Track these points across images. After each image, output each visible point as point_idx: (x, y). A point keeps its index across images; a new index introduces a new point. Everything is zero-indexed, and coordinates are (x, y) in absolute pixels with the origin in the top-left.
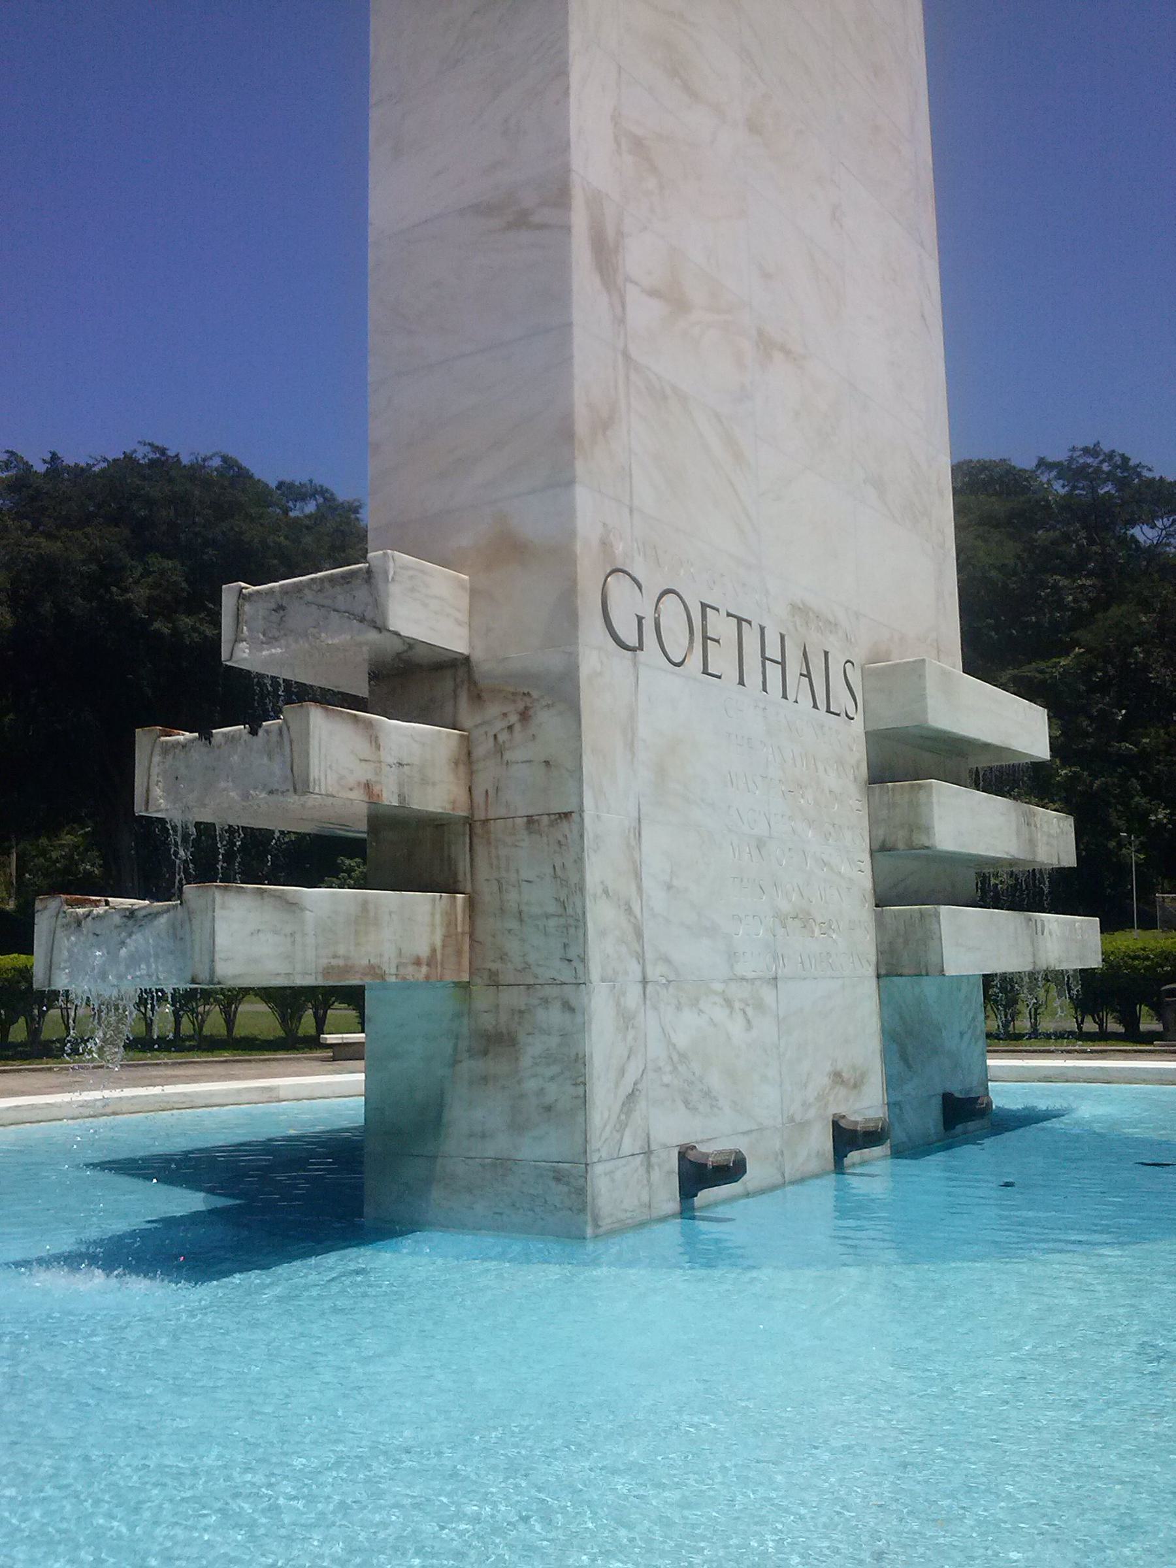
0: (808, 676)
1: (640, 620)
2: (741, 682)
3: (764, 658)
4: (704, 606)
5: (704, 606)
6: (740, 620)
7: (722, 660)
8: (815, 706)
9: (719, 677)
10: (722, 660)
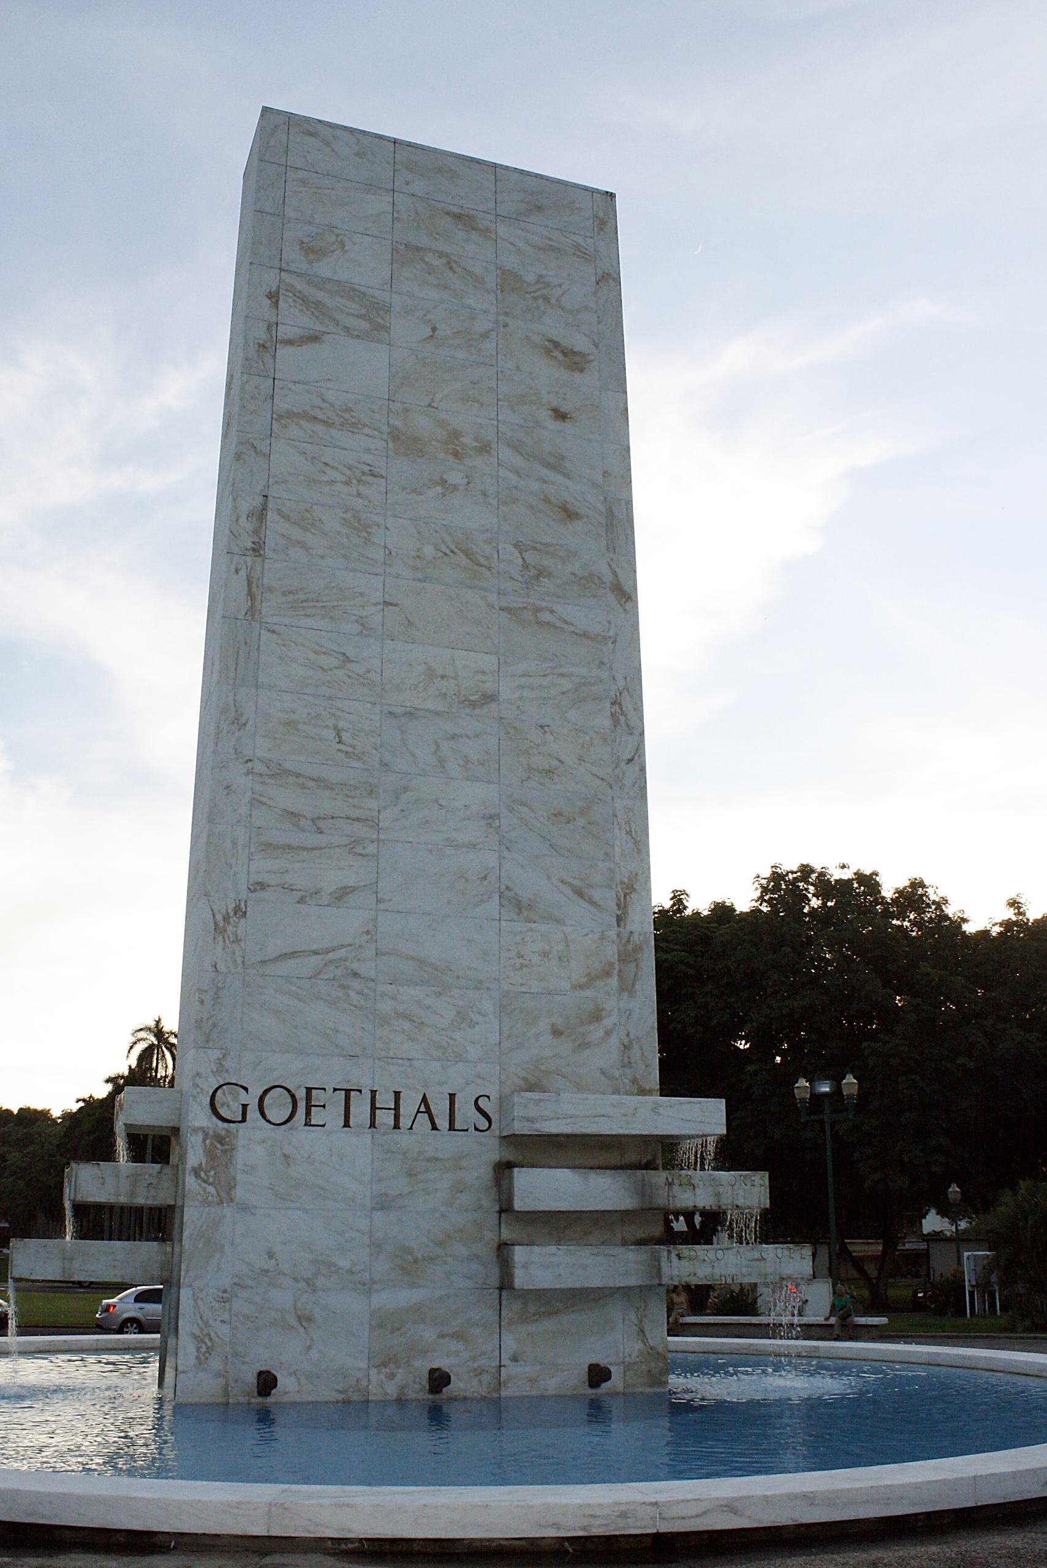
0: (428, 1111)
1: (245, 1106)
2: (347, 1124)
3: (373, 1108)
4: (309, 1090)
5: (309, 1090)
6: (348, 1092)
8: (434, 1127)
9: (323, 1126)
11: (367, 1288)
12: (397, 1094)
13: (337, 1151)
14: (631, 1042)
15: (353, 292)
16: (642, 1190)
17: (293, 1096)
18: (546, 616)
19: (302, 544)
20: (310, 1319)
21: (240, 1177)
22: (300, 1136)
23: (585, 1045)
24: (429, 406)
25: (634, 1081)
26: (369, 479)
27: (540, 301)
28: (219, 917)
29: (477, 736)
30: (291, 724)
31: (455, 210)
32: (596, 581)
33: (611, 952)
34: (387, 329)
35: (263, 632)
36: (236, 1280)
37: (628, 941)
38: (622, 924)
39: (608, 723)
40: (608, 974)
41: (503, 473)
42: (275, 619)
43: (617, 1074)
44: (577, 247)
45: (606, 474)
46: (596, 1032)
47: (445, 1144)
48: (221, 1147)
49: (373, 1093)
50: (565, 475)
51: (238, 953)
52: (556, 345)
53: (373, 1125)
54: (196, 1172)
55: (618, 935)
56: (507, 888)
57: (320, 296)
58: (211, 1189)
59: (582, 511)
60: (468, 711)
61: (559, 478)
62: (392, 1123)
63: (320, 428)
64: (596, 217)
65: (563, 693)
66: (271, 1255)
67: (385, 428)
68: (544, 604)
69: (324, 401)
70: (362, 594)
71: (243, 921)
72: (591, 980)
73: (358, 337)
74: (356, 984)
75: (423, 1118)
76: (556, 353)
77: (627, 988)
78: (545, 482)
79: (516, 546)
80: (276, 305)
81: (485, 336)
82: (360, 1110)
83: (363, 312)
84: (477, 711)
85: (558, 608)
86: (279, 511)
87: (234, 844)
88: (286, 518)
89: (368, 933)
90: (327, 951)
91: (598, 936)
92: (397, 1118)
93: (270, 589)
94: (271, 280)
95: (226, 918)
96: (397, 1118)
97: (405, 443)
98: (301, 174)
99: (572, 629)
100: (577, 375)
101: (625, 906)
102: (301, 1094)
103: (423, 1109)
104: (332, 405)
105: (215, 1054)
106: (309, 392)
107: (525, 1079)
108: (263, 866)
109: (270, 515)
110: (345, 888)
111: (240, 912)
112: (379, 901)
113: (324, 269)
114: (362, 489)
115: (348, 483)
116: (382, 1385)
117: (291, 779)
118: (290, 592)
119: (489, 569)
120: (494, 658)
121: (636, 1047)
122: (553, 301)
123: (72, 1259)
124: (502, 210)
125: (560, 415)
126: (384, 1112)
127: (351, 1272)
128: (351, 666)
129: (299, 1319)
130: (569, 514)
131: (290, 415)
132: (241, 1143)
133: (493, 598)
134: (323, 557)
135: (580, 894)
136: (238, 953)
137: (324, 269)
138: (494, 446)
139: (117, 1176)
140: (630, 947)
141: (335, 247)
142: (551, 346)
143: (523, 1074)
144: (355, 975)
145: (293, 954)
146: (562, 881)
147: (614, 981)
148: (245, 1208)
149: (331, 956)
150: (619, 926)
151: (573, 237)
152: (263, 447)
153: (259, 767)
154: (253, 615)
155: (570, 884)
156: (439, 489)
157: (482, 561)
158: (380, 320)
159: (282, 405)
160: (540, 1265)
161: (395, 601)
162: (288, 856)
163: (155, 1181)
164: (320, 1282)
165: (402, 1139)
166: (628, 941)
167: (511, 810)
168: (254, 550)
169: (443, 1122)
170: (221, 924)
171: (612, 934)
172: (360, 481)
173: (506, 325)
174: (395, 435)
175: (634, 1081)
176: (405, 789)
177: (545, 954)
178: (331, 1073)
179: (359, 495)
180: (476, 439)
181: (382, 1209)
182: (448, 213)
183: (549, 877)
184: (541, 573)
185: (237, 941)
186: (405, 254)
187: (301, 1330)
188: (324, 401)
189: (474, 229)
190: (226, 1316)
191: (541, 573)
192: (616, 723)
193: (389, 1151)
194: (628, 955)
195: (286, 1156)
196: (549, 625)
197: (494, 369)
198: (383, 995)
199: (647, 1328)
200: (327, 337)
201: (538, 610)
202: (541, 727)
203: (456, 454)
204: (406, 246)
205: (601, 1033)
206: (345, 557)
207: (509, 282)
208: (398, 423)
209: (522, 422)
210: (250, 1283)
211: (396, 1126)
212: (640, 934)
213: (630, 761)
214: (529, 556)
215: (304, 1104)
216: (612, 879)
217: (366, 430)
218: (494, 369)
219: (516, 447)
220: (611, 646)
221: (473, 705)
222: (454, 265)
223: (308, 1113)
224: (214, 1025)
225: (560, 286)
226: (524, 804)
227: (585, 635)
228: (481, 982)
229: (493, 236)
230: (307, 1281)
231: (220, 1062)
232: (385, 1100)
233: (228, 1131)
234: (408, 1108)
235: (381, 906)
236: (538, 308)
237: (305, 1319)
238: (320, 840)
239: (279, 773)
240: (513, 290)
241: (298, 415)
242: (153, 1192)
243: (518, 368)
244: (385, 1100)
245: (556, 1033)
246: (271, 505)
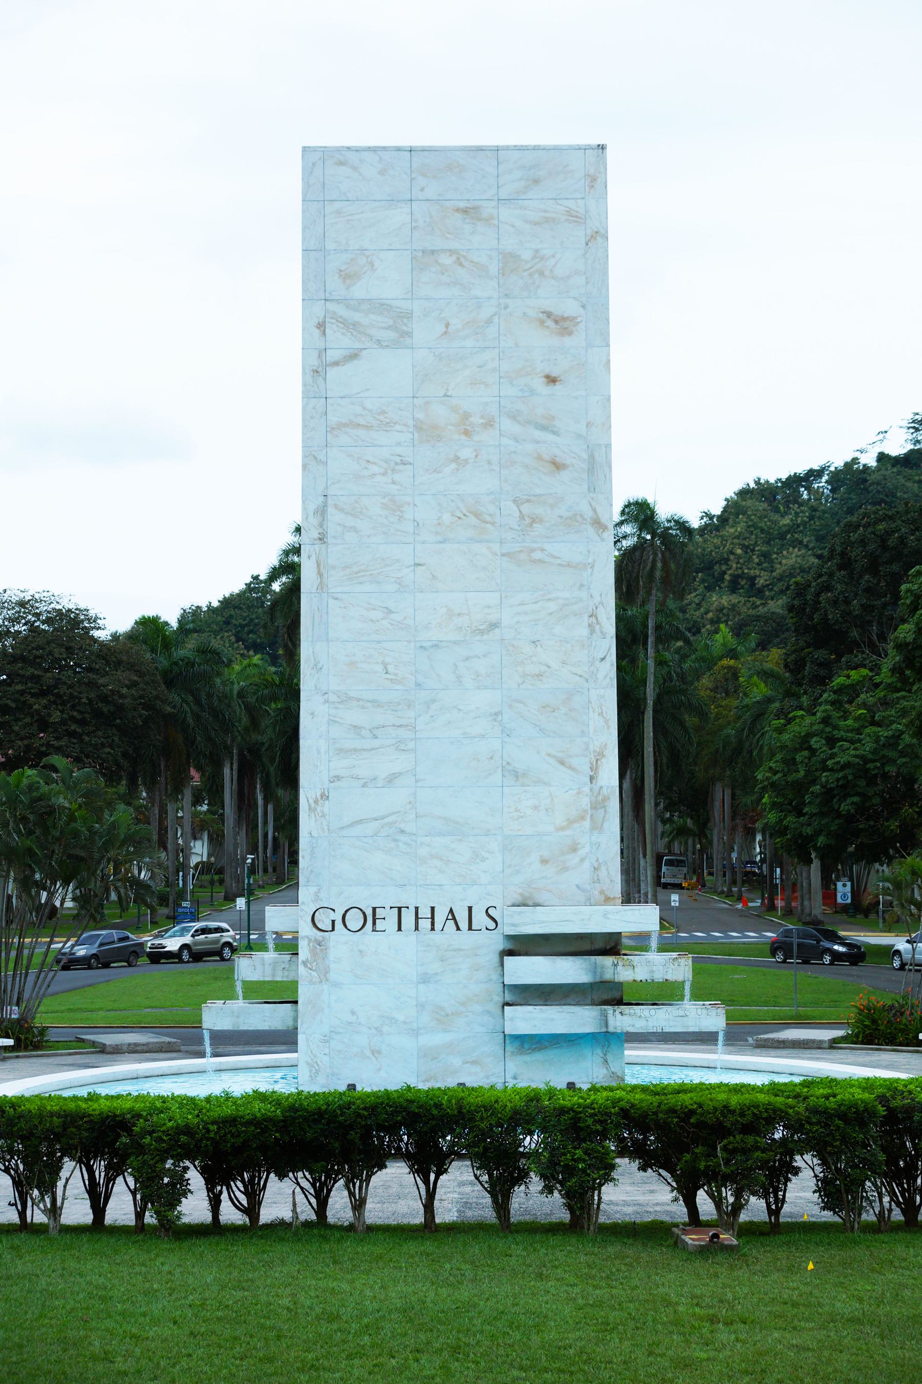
0: (454, 918)
1: (333, 922)
2: (400, 929)
3: (417, 918)
5: (374, 909)
6: (400, 909)
7: (388, 923)
8: (458, 929)
10: (388, 923)
11: (416, 1033)
12: (433, 909)
13: (393, 947)
14: (599, 865)
15: (381, 307)
16: (594, 969)
17: (364, 913)
18: (537, 555)
19: (354, 529)
20: (379, 1052)
21: (332, 966)
23: (566, 869)
24: (445, 395)
25: (602, 892)
26: (401, 467)
27: (536, 276)
28: (311, 801)
29: (484, 656)
30: (352, 664)
31: (462, 205)
32: (579, 518)
33: (585, 802)
34: (409, 334)
35: (331, 601)
36: (332, 1029)
37: (599, 793)
38: (594, 781)
39: (585, 632)
40: (583, 818)
41: (505, 441)
42: (339, 589)
43: (588, 887)
44: (569, 213)
45: (588, 425)
46: (573, 860)
47: (465, 938)
49: (417, 908)
50: (554, 433)
51: (325, 823)
52: (549, 314)
53: (417, 928)
54: (305, 963)
55: (591, 790)
56: (508, 763)
57: (357, 317)
58: (314, 974)
59: (568, 462)
60: (478, 638)
61: (550, 437)
62: (429, 927)
63: (361, 432)
64: (587, 175)
65: (551, 614)
66: (353, 1013)
67: (411, 423)
68: (535, 546)
69: (364, 408)
70: (398, 561)
71: (327, 802)
72: (571, 822)
73: (387, 346)
74: (403, 838)
75: (451, 923)
76: (550, 323)
77: (597, 827)
78: (538, 442)
79: (514, 501)
80: (324, 333)
81: (489, 321)
82: (408, 919)
83: (391, 323)
84: (485, 637)
85: (546, 546)
86: (336, 506)
87: (319, 752)
88: (341, 510)
89: (410, 803)
90: (383, 818)
91: (575, 792)
92: (433, 924)
93: (334, 567)
94: (318, 310)
95: (316, 802)
96: (433, 924)
97: (427, 432)
98: (337, 205)
99: (558, 561)
100: (567, 341)
101: (597, 768)
102: (369, 913)
103: (450, 917)
104: (370, 411)
105: (313, 889)
106: (353, 404)
107: (521, 894)
109: (330, 510)
110: (394, 774)
111: (325, 797)
112: (417, 781)
114: (397, 477)
115: (384, 474)
117: (354, 703)
118: (347, 567)
119: (493, 524)
120: (497, 595)
121: (603, 869)
122: (547, 273)
123: (238, 1017)
124: (503, 194)
125: (552, 380)
127: (405, 1023)
128: (392, 616)
129: (373, 1052)
130: (557, 466)
131: (341, 426)
132: (331, 944)
133: (496, 547)
134: (369, 536)
135: (562, 763)
136: (325, 823)
137: (358, 291)
138: (497, 420)
139: (264, 965)
140: (600, 798)
141: (366, 268)
142: (544, 317)
143: (520, 891)
144: (402, 831)
145: (360, 822)
146: (549, 755)
147: (587, 823)
148: (337, 985)
149: (386, 820)
150: (591, 783)
151: (566, 203)
152: (322, 457)
153: (333, 698)
154: (322, 589)
155: (554, 756)
156: (454, 466)
157: (488, 519)
158: (404, 328)
159: (333, 419)
161: (421, 562)
162: (354, 756)
163: (287, 966)
164: (385, 1029)
165: (436, 936)
166: (599, 793)
167: (510, 707)
168: (320, 539)
169: (464, 925)
170: (313, 805)
171: (586, 789)
172: (393, 470)
173: (506, 307)
174: (419, 427)
175: (602, 892)
176: (434, 701)
177: (536, 808)
178: (387, 898)
179: (393, 482)
180: (482, 417)
181: (424, 982)
182: (458, 210)
183: (538, 753)
184: (534, 520)
185: (323, 816)
186: (424, 258)
187: (374, 1059)
188: (364, 408)
189: (480, 219)
190: (327, 1051)
191: (534, 520)
192: (592, 632)
193: (428, 945)
194: (598, 805)
195: (361, 951)
196: (541, 561)
197: (497, 351)
198: (422, 844)
199: (610, 1058)
200: (364, 353)
201: (533, 550)
202: (534, 642)
203: (466, 433)
204: (423, 252)
205: (577, 860)
206: (385, 533)
207: (510, 262)
208: (420, 416)
209: (520, 394)
210: (340, 1030)
211: (433, 929)
212: (608, 788)
213: (602, 659)
214: (525, 508)
215: (371, 918)
216: (587, 749)
217: (398, 427)
218: (497, 351)
219: (514, 417)
220: (590, 571)
221: (482, 632)
222: (462, 260)
223: (374, 923)
224: (312, 872)
225: (553, 256)
226: (520, 702)
227: (569, 565)
228: (489, 830)
229: (496, 222)
230: (376, 1029)
231: (317, 894)
232: (425, 912)
233: (323, 937)
234: (440, 918)
235: (419, 784)
236: (534, 283)
237: (376, 1052)
238: (376, 743)
239: (345, 699)
240: (512, 271)
241: (345, 425)
242: (286, 973)
243: (517, 345)
244: (425, 912)
245: (544, 861)
246: (330, 501)
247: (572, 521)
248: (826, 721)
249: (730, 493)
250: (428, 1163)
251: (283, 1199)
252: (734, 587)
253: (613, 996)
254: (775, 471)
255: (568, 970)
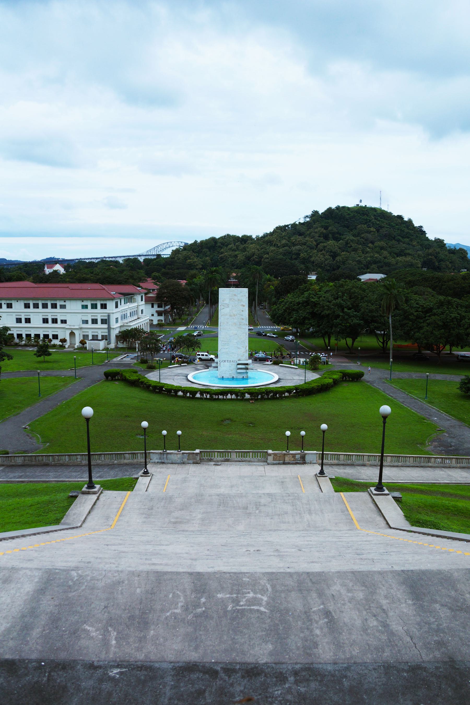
15: (226, 304)
22: (225, 363)
48: (220, 364)
97: (230, 316)
108: (222, 347)
113: (224, 302)
116: (230, 377)
126: (229, 361)
137: (224, 302)
160: (239, 371)
178: (226, 359)
186: (230, 299)
207: (239, 300)
215: (225, 361)
247: (244, 324)
248: (278, 307)
249: (275, 227)
250: (231, 395)
251: (221, 397)
252: (274, 245)
253: (247, 369)
254: (282, 224)
255: (243, 366)
